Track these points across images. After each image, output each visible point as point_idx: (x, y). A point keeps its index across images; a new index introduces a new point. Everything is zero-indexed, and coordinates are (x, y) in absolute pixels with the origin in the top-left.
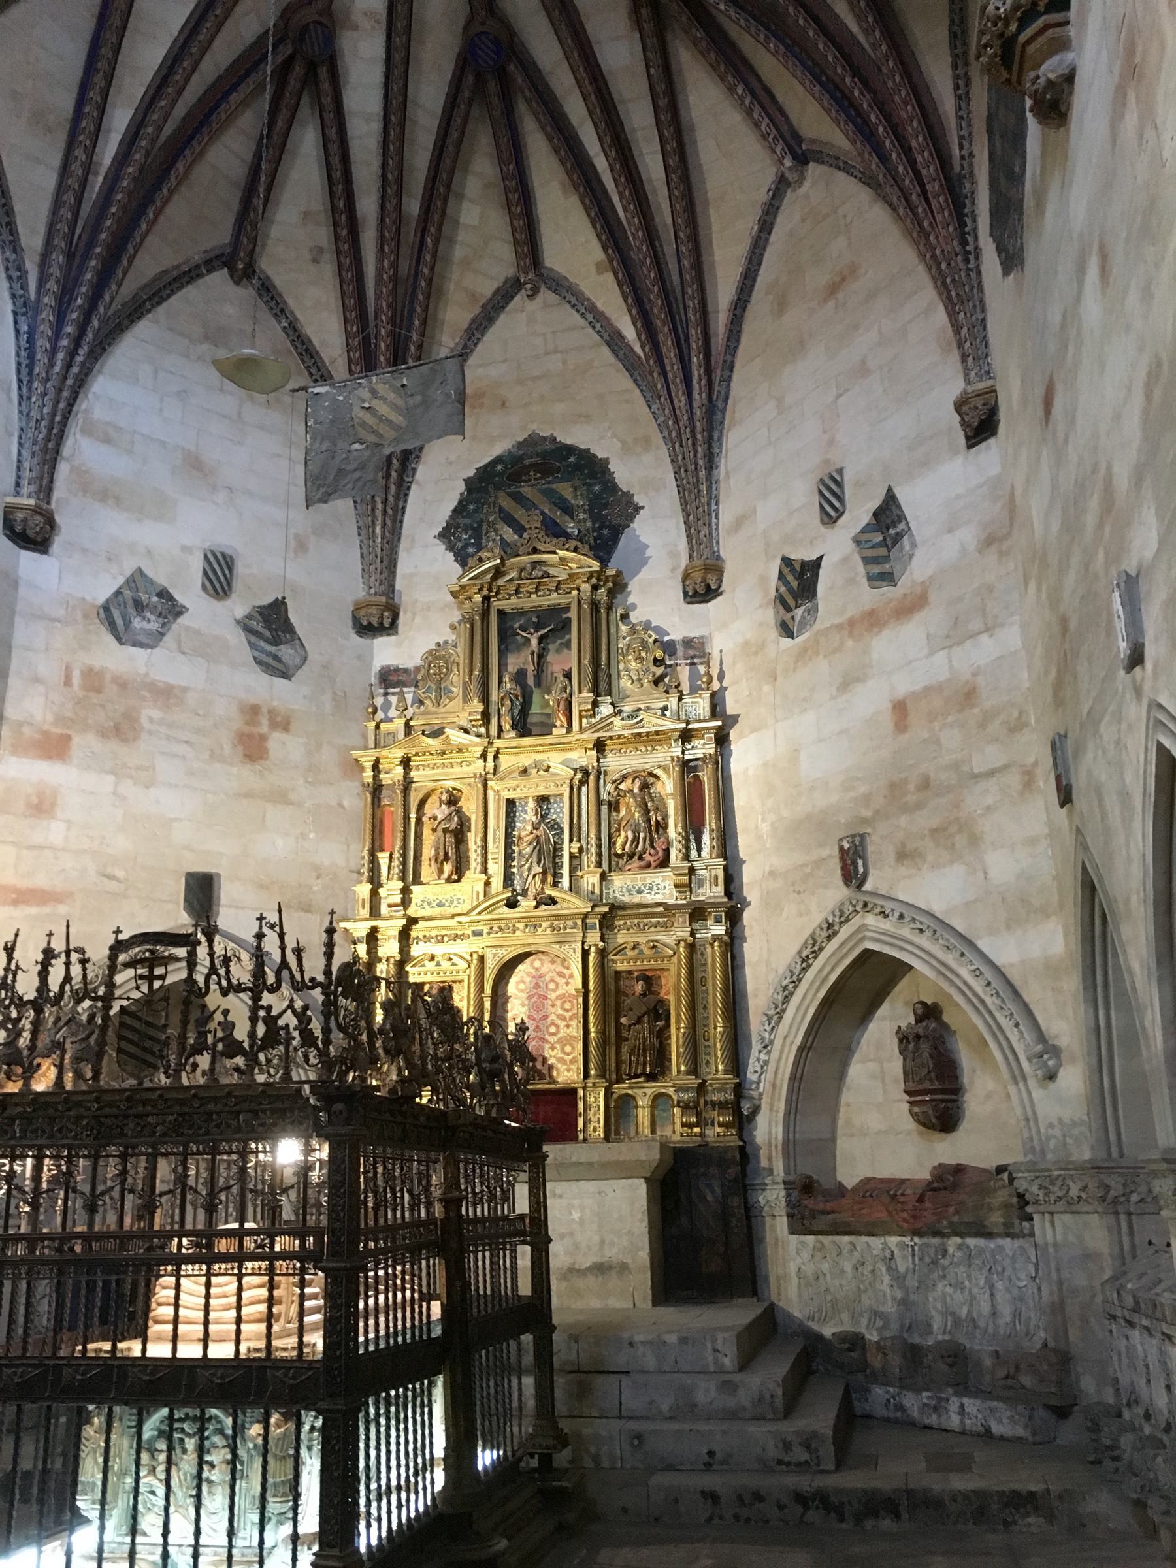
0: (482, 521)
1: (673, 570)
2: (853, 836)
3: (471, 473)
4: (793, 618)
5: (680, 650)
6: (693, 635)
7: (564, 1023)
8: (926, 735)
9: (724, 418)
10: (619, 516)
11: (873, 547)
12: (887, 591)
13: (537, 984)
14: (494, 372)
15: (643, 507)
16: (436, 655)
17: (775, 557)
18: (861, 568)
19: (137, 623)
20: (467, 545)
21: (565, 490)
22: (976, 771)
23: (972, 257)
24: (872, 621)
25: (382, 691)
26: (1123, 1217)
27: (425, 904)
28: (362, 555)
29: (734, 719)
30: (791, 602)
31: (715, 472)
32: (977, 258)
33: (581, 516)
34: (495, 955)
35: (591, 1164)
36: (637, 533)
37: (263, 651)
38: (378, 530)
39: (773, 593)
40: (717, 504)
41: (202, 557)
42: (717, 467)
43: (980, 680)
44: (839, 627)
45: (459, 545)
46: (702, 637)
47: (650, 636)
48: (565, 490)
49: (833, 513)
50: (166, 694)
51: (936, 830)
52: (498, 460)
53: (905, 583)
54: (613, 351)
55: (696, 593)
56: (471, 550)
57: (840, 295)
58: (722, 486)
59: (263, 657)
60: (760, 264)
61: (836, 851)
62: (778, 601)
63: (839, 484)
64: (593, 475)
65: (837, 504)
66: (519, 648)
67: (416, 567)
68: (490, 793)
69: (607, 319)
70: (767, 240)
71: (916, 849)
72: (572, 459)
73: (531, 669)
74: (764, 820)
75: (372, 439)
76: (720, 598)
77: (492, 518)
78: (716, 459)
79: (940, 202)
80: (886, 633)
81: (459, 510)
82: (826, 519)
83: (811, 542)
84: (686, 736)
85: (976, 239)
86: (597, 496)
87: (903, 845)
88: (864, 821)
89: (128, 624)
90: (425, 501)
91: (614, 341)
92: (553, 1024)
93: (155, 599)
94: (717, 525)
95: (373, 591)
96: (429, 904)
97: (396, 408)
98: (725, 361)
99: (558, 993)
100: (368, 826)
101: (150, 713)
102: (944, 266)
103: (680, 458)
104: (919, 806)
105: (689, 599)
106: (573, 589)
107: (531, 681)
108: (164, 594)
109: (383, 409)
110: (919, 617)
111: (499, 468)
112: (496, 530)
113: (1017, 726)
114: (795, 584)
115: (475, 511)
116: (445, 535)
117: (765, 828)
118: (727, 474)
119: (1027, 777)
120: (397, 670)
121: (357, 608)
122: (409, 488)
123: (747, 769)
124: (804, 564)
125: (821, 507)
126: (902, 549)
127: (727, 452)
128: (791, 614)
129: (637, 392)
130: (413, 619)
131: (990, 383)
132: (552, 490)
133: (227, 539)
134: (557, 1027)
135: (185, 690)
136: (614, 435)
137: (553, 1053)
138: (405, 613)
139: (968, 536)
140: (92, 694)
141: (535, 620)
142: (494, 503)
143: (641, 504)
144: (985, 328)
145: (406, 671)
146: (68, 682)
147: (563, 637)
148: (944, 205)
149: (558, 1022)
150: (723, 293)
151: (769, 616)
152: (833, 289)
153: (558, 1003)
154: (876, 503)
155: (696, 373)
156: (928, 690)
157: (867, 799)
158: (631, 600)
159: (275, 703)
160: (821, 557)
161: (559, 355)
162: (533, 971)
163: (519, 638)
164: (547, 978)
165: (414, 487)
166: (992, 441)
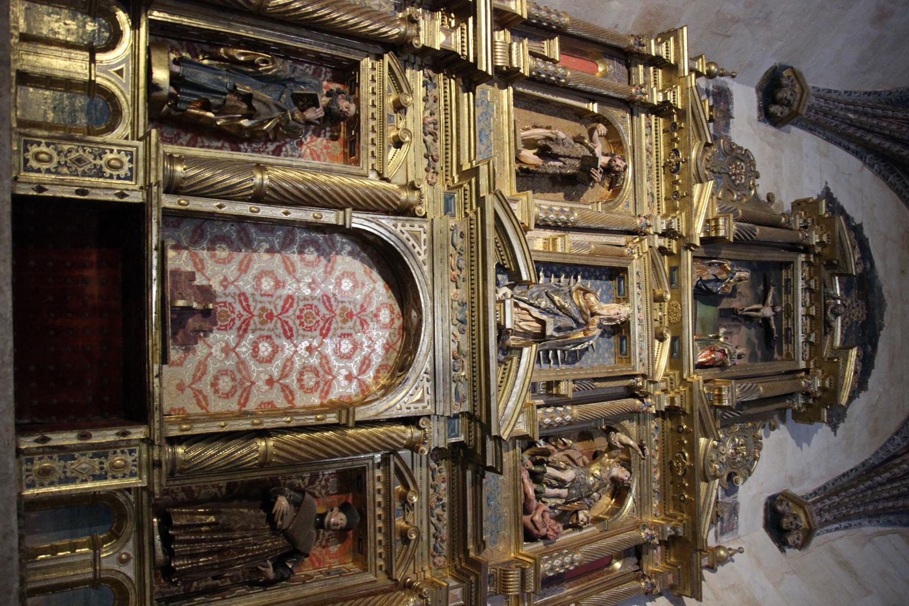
6: (740, 514)
7: (276, 375)
13: (350, 315)
25: (711, 88)
36: (819, 430)
40: (846, 528)
46: (737, 528)
68: (622, 240)
73: (735, 304)
76: (773, 547)
92: (276, 350)
94: (830, 531)
99: (333, 358)
100: (586, 35)
107: (725, 304)
116: (827, 194)
121: (797, 76)
122: (861, 158)
134: (270, 360)
137: (216, 351)
138: (774, 134)
143: (838, 431)
149: (278, 362)
153: (314, 361)
162: (373, 308)
164: (358, 336)
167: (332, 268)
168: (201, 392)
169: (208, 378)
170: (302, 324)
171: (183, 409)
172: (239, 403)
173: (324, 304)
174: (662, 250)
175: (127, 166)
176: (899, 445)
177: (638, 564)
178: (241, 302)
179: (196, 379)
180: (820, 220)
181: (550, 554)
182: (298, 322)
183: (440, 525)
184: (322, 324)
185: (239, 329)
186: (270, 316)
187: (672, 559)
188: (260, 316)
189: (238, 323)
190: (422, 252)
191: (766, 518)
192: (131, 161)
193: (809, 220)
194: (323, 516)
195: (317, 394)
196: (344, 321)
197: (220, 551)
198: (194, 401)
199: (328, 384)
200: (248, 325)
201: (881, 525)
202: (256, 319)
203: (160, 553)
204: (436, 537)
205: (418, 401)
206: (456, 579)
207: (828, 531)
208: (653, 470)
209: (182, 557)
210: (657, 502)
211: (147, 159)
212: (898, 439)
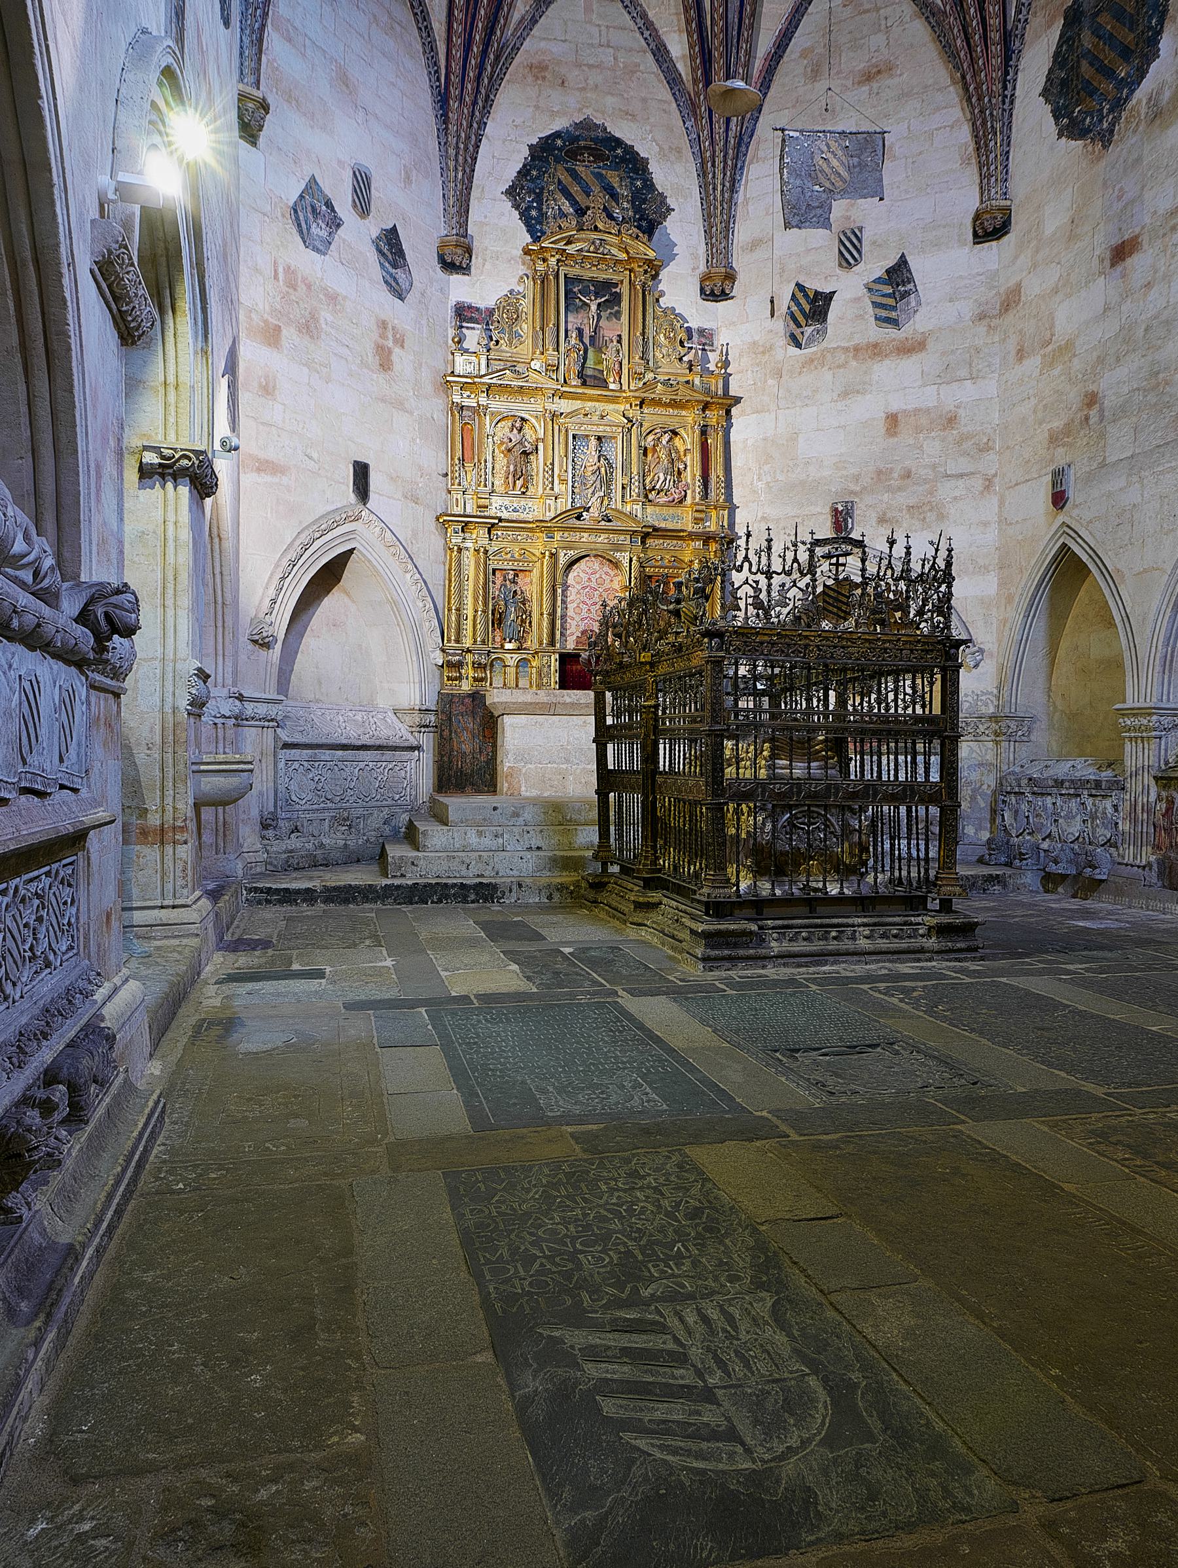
0: (542, 189)
1: (694, 269)
2: (846, 502)
3: (535, 141)
4: (802, 333)
8: (911, 442)
10: (655, 213)
11: (883, 296)
12: (891, 332)
14: (556, 49)
15: (673, 210)
16: (510, 301)
17: (789, 282)
18: (870, 309)
19: (315, 230)
20: (529, 208)
21: (613, 178)
22: (948, 473)
23: (1007, 101)
24: (876, 351)
26: (1012, 743)
27: (503, 508)
29: (738, 400)
30: (802, 321)
31: (735, 196)
32: (1012, 102)
33: (625, 205)
37: (387, 272)
38: (460, 175)
41: (352, 173)
42: (737, 192)
43: (961, 412)
44: (846, 349)
45: (523, 205)
47: (678, 321)
48: (613, 178)
49: (852, 261)
50: (333, 298)
51: (912, 507)
52: (557, 135)
53: (907, 331)
54: (657, 60)
55: (712, 293)
56: (534, 213)
57: (875, 85)
58: (739, 209)
59: (388, 278)
60: (796, 28)
61: (827, 510)
62: (788, 317)
63: (859, 240)
64: (635, 170)
65: (856, 255)
66: (577, 310)
69: (656, 30)
70: (806, 9)
71: (894, 518)
72: (619, 151)
73: (587, 333)
74: (759, 479)
75: (828, 185)
77: (552, 188)
79: (996, 49)
80: (887, 362)
81: (523, 173)
82: (845, 264)
83: (826, 277)
84: (706, 407)
85: (1014, 88)
86: (638, 190)
87: (884, 514)
88: (852, 492)
89: (308, 229)
90: (493, 157)
91: (660, 53)
93: (324, 208)
95: (454, 232)
96: (506, 509)
97: (842, 163)
101: (325, 315)
102: (986, 99)
103: (710, 176)
104: (899, 489)
105: (703, 296)
106: (626, 269)
107: (587, 341)
108: (329, 204)
109: (835, 163)
110: (916, 358)
111: (559, 142)
112: (555, 200)
113: (986, 448)
114: (807, 308)
115: (537, 178)
116: (511, 192)
118: (746, 200)
119: (987, 483)
120: (470, 307)
124: (817, 293)
125: (840, 252)
126: (908, 303)
127: (747, 181)
128: (801, 330)
129: (674, 105)
131: (1008, 203)
132: (601, 175)
133: (370, 164)
135: (345, 298)
136: (654, 140)
139: (966, 308)
140: (291, 291)
141: (592, 288)
142: (554, 175)
144: (1008, 159)
145: (478, 309)
146: (276, 277)
148: (999, 54)
150: (765, 43)
151: (779, 326)
152: (868, 77)
154: (890, 263)
156: (917, 411)
157: (857, 478)
158: (661, 287)
159: (396, 322)
160: (835, 292)
161: (611, 50)
163: (577, 300)
166: (994, 243)
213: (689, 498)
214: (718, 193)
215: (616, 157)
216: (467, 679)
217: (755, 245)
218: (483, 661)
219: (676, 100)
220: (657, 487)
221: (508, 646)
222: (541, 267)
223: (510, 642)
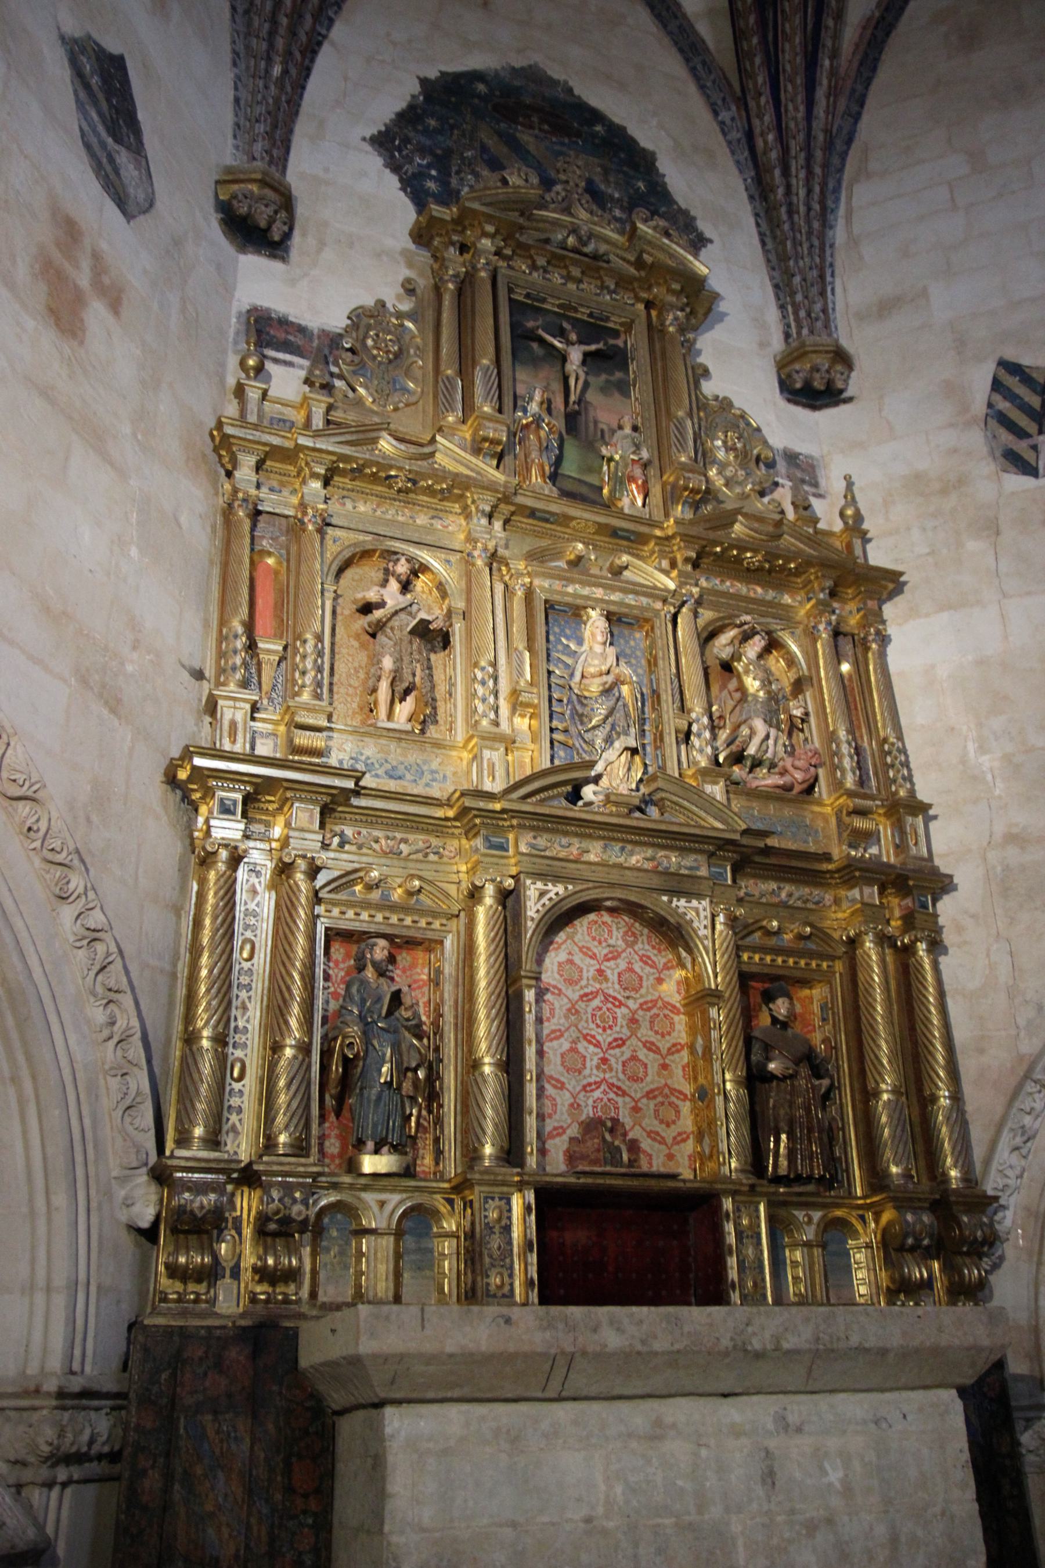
3: (432, 74)
4: (1035, 448)
5: (781, 466)
9: (843, 165)
15: (711, 241)
28: (237, 100)
31: (830, 233)
34: (542, 894)
35: (883, 1352)
39: (979, 406)
40: (833, 275)
42: (831, 227)
45: (409, 169)
46: (812, 457)
62: (993, 423)
67: (327, 170)
72: (598, 128)
76: (843, 408)
78: (831, 217)
81: (409, 117)
98: (853, 90)
111: (481, 87)
115: (439, 131)
116: (382, 142)
117: (986, 762)
118: (854, 242)
120: (283, 322)
123: (933, 666)
128: (1031, 442)
130: (319, 251)
138: (304, 235)
145: (302, 330)
147: (612, 374)
155: (825, 82)
165: (326, 48)
167: (555, 987)
168: (674, 1138)
169: (660, 1128)
170: (610, 1027)
171: (690, 1157)
172: (684, 1100)
173: (589, 1000)
174: (506, 522)
175: (497, 1202)
176: (733, 119)
177: (845, 635)
178: (592, 1091)
179: (663, 1142)
180: (460, 223)
181: (834, 767)
182: (609, 1031)
183: (797, 895)
184: (610, 1005)
185: (617, 1094)
186: (604, 1060)
187: (850, 591)
188: (604, 1071)
189: (612, 1095)
190: (555, 890)
191: (805, 406)
192: (493, 1199)
193: (455, 238)
194: (775, 1020)
195: (676, 1018)
196: (606, 979)
197: (810, 1130)
198: (682, 1145)
199: (666, 1005)
200: (613, 1085)
201: (837, 207)
202: (607, 1076)
203: (811, 1188)
204: (806, 901)
205: (698, 914)
206: (852, 887)
207: (834, 309)
208: (752, 594)
209: (812, 1169)
210: (786, 597)
211: (495, 1183)
212: (725, 115)
213: (822, 788)
214: (800, 220)
215: (594, 135)
216: (236, 1273)
217: (885, 308)
218: (297, 1211)
219: (697, 78)
220: (751, 750)
221: (370, 1163)
222: (456, 263)
223: (377, 1151)
